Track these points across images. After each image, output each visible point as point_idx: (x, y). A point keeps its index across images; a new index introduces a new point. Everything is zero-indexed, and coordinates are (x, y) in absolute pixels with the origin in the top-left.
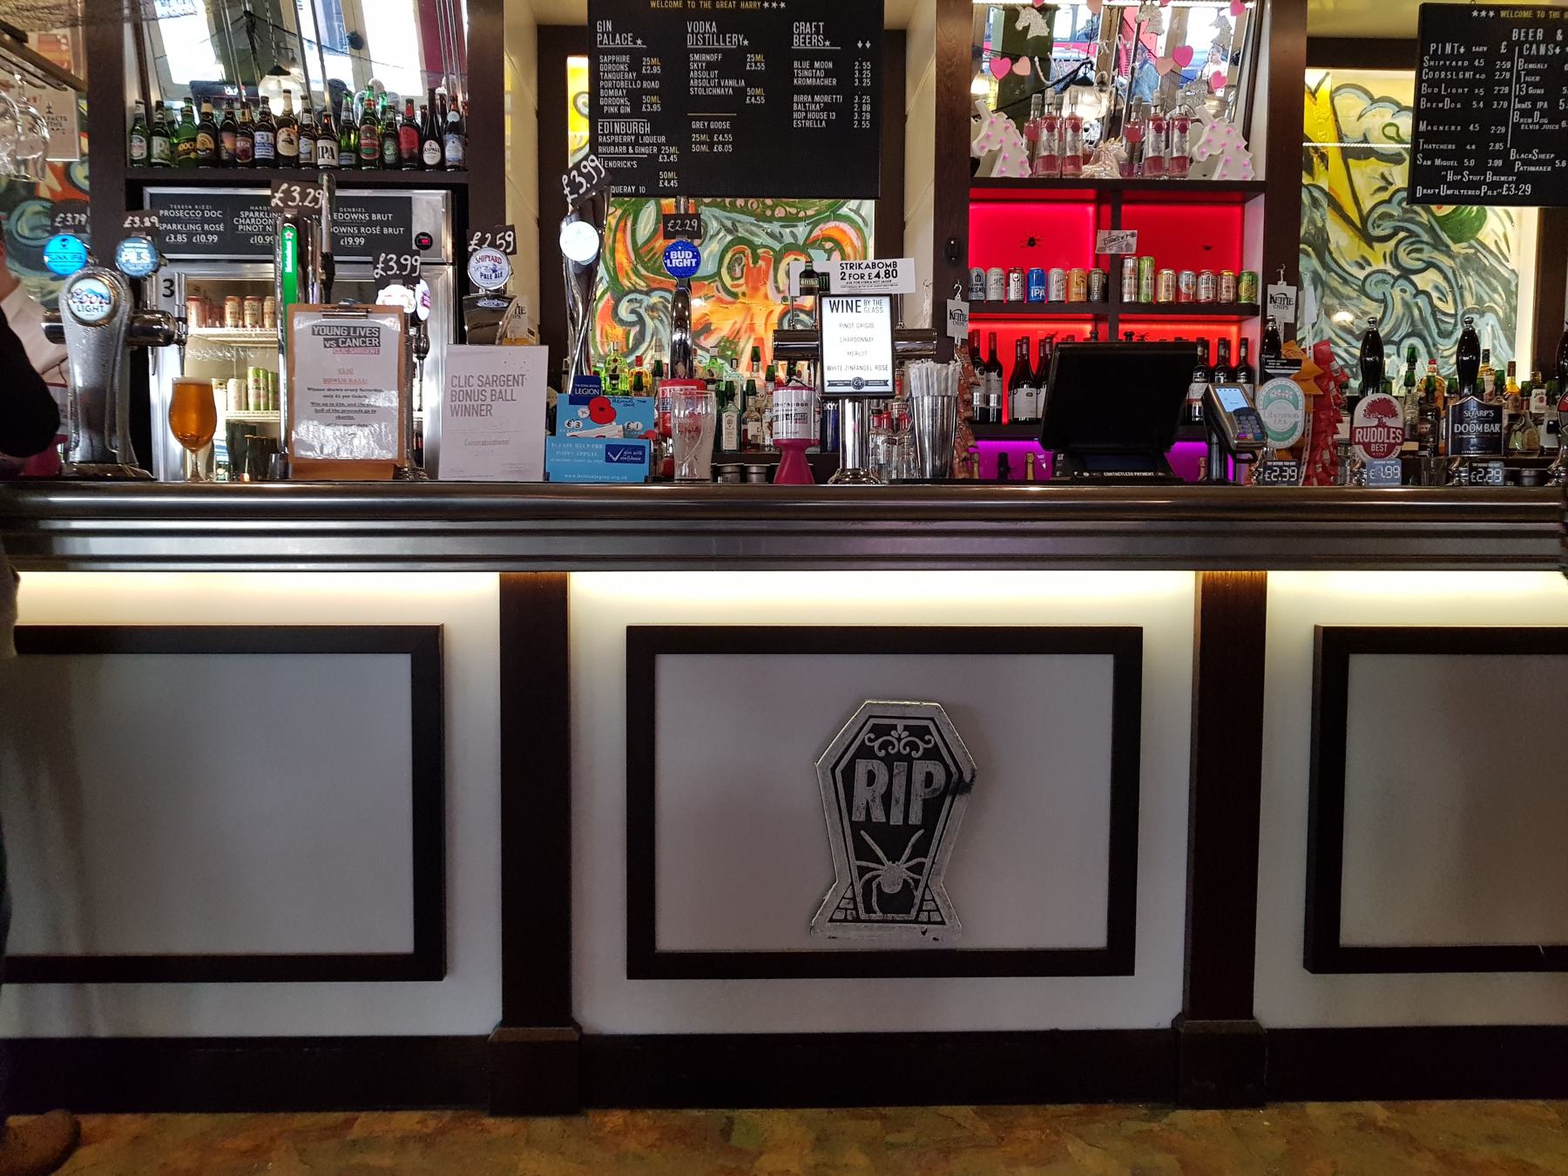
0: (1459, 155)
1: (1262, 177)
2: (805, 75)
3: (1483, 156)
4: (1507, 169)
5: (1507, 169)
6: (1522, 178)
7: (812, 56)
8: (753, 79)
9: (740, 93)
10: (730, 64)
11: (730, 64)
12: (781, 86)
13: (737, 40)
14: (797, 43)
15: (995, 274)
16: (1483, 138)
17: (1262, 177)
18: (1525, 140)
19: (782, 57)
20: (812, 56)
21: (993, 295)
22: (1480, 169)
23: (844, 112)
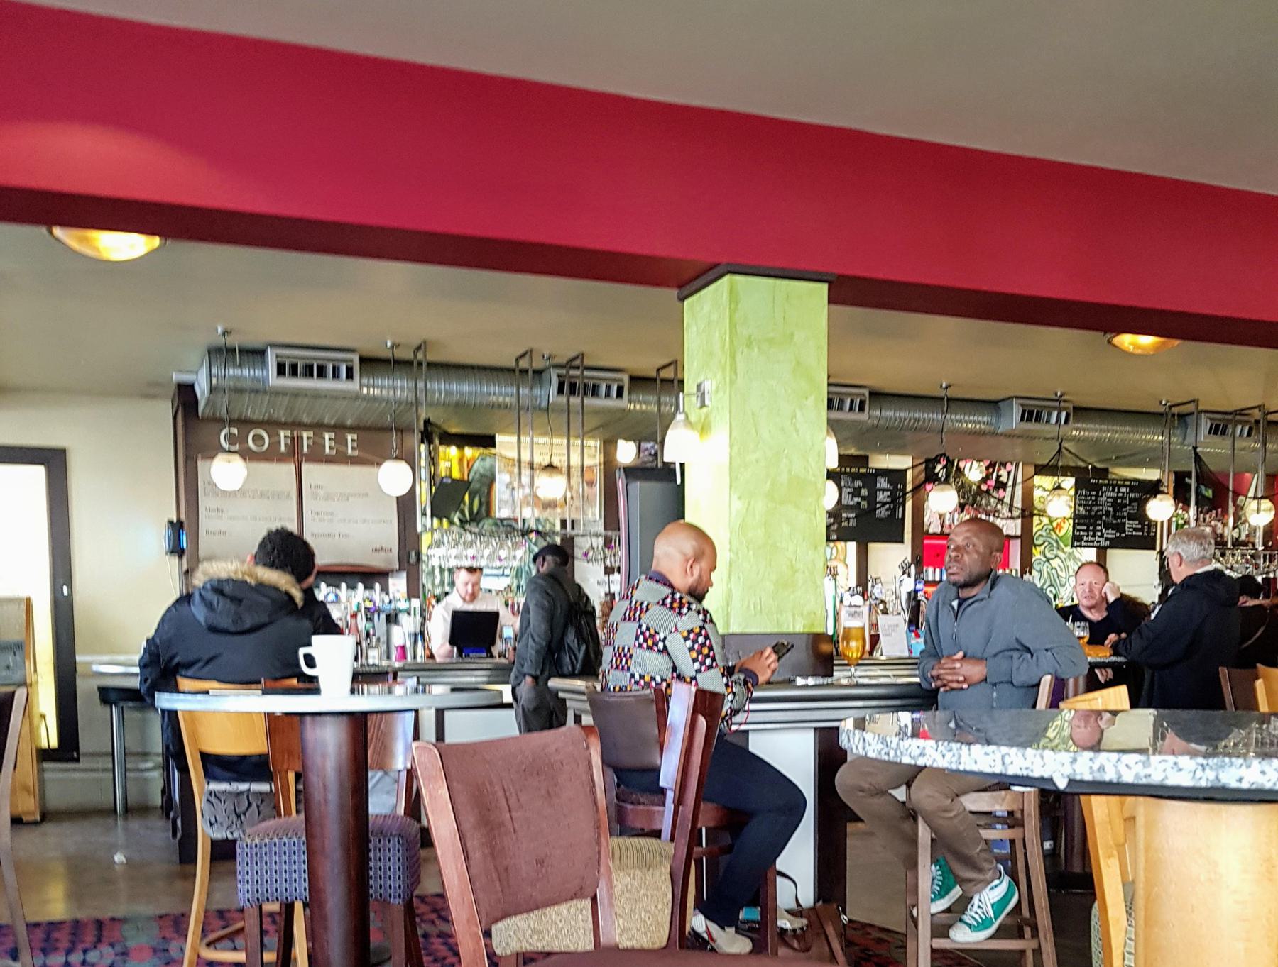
0: (1087, 530)
1: (1019, 533)
2: (881, 497)
3: (1095, 531)
4: (1102, 536)
5: (1102, 536)
6: (1107, 539)
7: (884, 490)
8: (863, 498)
9: (859, 504)
10: (856, 492)
11: (856, 492)
12: (872, 498)
13: (858, 483)
14: (878, 485)
15: (931, 570)
16: (1095, 525)
17: (1019, 533)
18: (1107, 526)
19: (873, 491)
20: (884, 490)
21: (930, 578)
22: (1094, 536)
23: (894, 511)
